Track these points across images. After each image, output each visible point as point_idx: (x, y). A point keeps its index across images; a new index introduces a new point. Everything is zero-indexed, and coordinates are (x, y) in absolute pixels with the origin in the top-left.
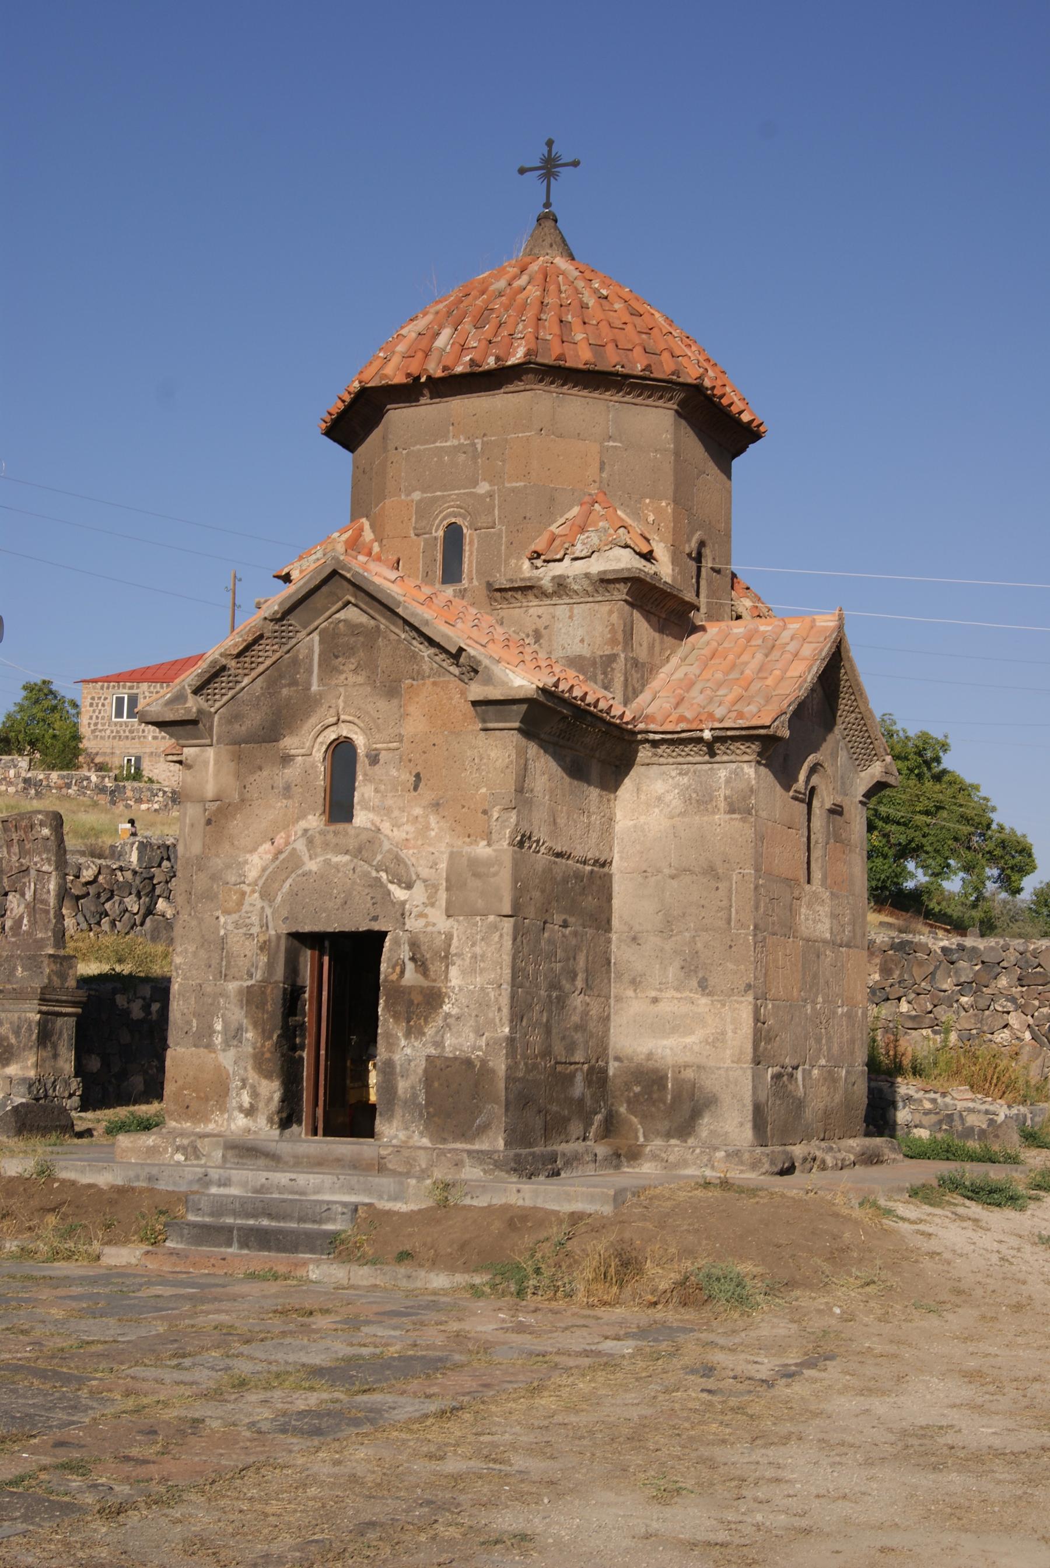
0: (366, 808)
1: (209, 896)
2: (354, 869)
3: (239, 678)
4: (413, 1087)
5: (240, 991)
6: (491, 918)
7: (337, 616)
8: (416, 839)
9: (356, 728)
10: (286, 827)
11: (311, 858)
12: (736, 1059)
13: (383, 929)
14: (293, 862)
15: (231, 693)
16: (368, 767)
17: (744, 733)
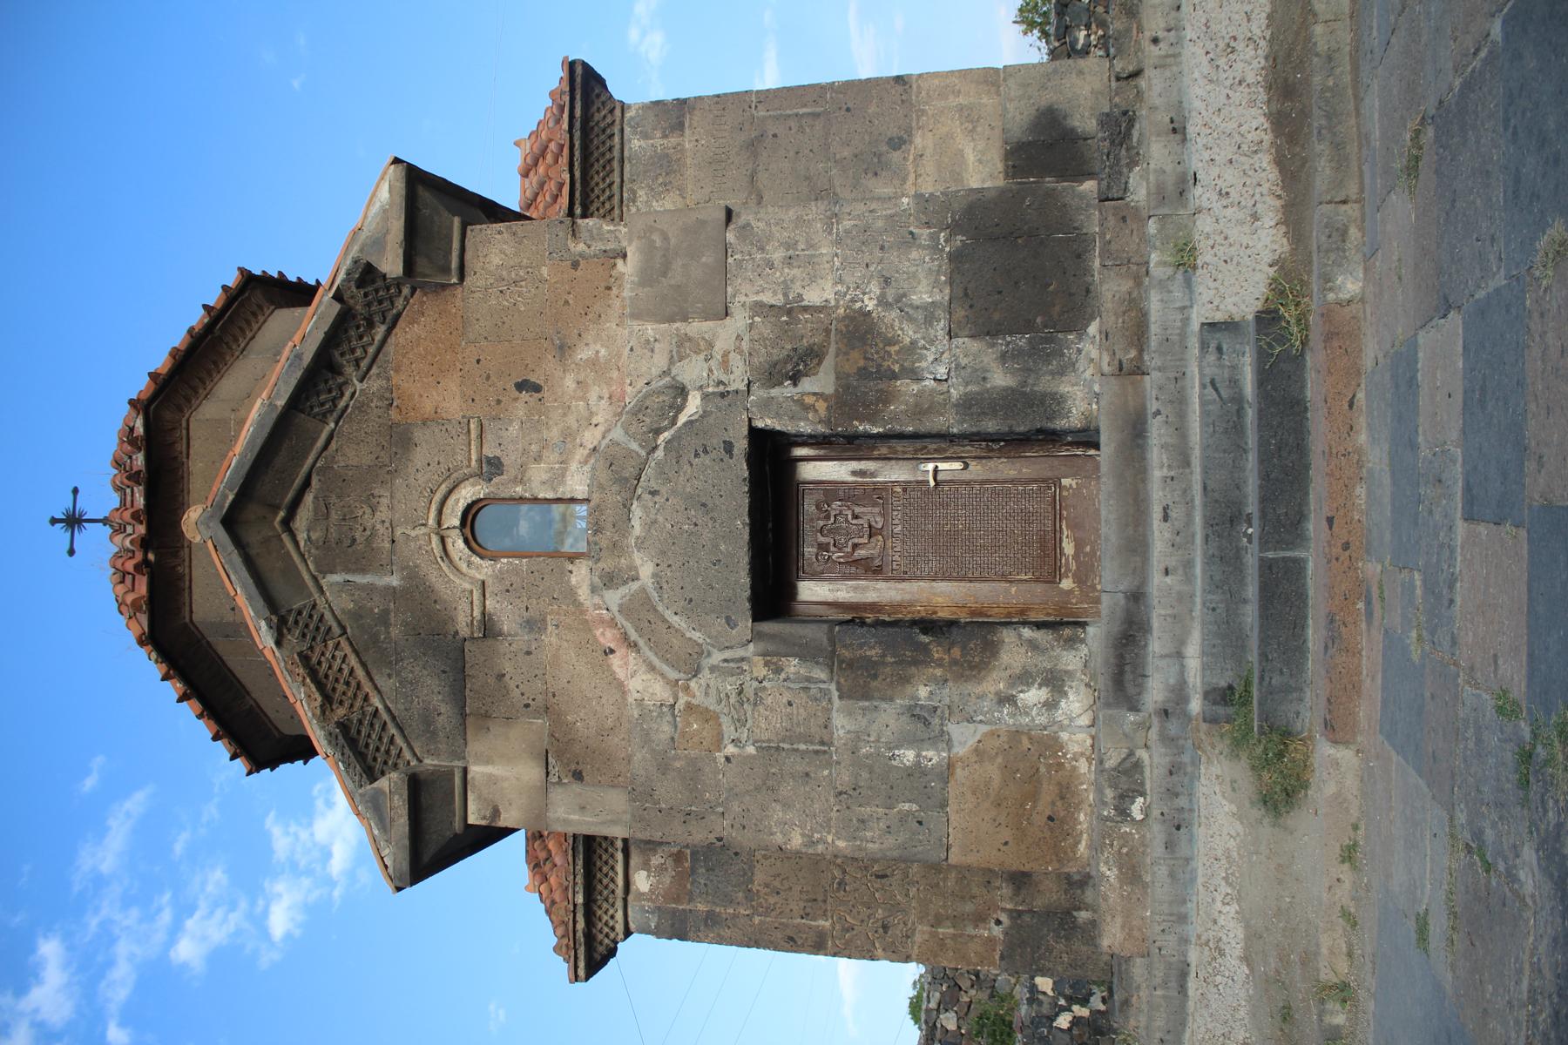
0: (559, 477)
1: (693, 776)
2: (654, 493)
3: (370, 709)
4: (1003, 357)
5: (850, 714)
6: (730, 236)
7: (302, 544)
8: (609, 382)
9: (450, 502)
10: (586, 627)
11: (635, 578)
12: (993, 90)
13: (745, 431)
14: (639, 608)
15: (393, 730)
16: (504, 477)
17: (578, 97)
